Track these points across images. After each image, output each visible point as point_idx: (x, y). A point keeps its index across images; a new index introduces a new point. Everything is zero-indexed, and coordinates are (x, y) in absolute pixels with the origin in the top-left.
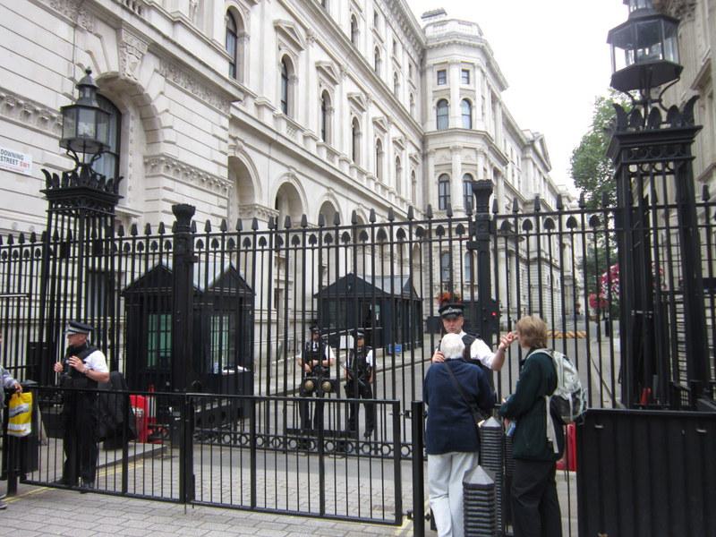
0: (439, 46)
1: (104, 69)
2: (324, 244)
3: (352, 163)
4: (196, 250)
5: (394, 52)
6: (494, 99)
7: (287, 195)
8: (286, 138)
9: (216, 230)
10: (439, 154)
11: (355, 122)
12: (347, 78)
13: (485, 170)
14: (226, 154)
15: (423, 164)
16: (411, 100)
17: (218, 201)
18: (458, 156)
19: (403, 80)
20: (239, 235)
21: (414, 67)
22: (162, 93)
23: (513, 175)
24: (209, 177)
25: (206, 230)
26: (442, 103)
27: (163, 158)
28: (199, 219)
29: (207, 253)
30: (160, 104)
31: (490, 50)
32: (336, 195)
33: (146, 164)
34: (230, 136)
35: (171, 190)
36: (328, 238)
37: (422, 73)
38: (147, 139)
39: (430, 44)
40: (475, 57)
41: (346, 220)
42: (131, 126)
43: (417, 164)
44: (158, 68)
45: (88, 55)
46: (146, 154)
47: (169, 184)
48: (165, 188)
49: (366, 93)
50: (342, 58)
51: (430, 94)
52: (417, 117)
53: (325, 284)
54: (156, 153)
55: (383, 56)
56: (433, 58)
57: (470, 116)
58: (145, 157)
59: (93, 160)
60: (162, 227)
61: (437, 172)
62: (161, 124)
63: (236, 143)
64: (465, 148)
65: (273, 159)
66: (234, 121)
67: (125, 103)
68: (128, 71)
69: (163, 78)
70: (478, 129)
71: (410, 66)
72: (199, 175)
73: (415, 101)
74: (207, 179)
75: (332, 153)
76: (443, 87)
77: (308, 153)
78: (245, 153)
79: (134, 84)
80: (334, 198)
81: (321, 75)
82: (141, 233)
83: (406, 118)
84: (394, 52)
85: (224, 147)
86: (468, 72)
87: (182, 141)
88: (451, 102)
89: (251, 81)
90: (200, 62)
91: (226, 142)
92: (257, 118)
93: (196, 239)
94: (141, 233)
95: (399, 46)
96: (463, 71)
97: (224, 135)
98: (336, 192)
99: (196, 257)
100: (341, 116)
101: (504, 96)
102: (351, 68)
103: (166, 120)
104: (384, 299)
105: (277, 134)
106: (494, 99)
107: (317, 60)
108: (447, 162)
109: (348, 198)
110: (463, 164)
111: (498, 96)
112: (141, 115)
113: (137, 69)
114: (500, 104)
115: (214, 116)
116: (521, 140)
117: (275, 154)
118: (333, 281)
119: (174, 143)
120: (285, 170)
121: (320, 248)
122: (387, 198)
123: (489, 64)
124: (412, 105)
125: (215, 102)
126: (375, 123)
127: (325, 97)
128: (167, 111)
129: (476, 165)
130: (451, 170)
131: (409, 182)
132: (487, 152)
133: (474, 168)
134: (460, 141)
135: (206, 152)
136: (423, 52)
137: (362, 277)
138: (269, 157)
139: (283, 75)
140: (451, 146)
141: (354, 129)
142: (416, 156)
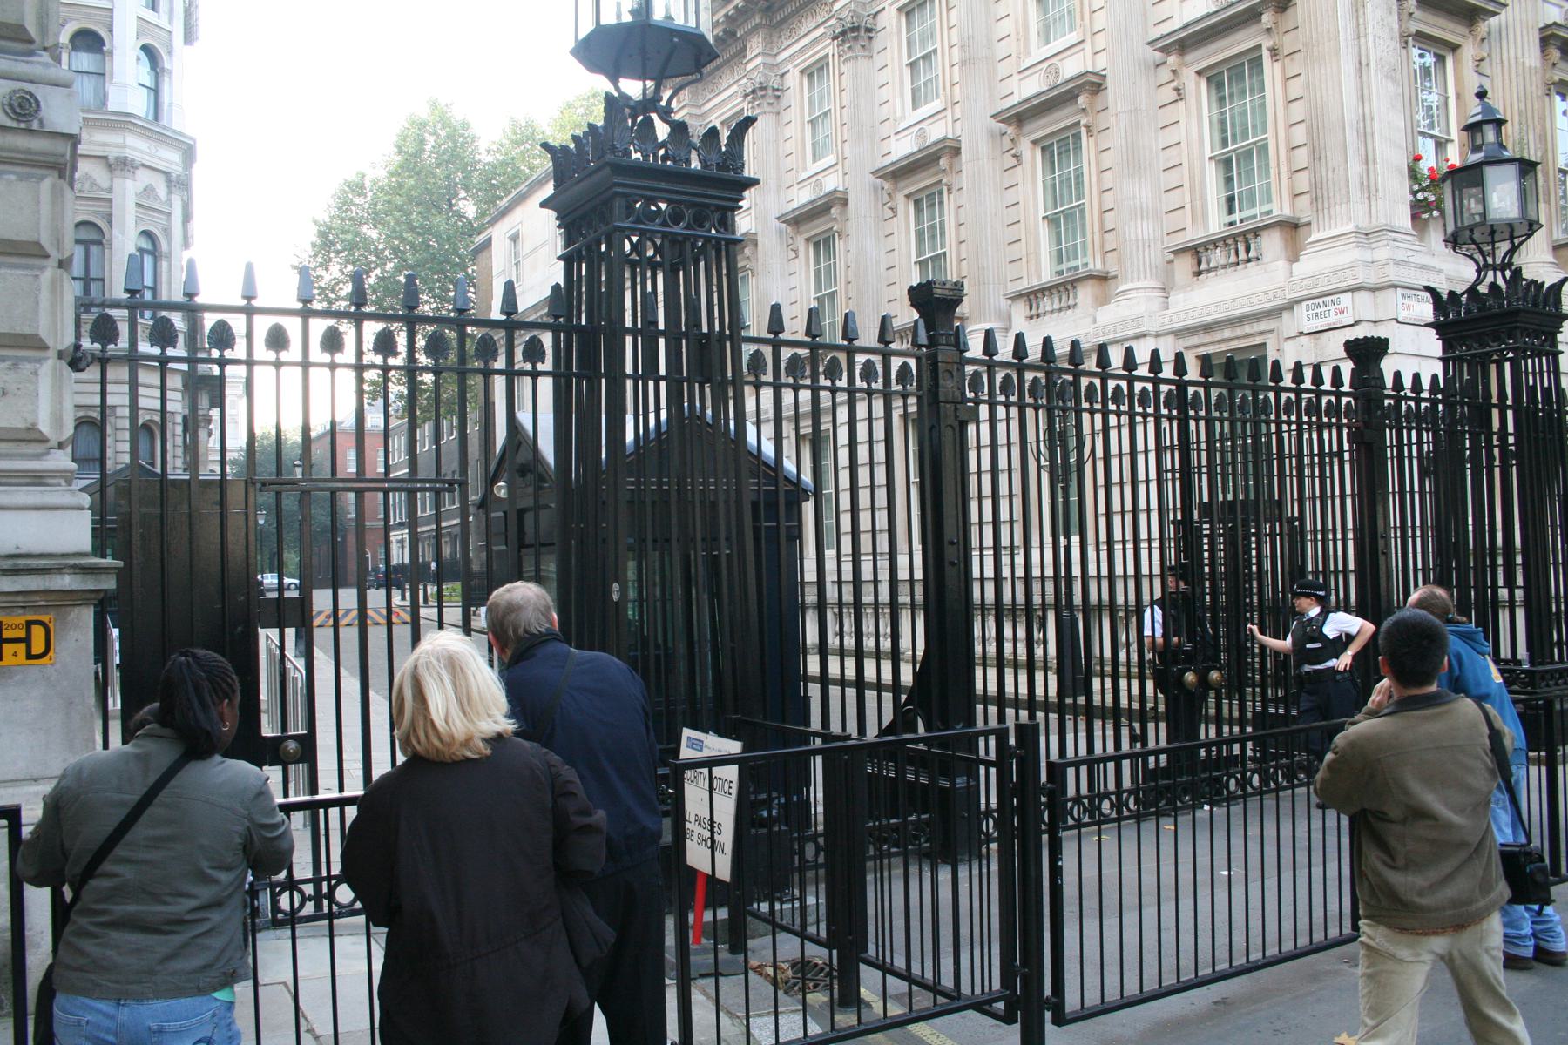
18: (129, 183)
64: (144, 166)
110: (138, 205)
129: (169, 215)
130: (109, 219)
133: (162, 219)
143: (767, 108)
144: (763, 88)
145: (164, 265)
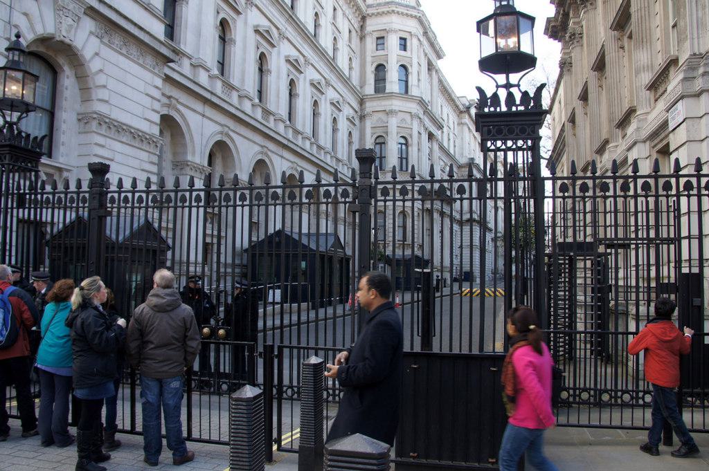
0: (378, 13)
1: (40, 31)
2: (223, 203)
3: (288, 122)
4: (109, 205)
5: (334, 17)
6: (431, 67)
7: (220, 150)
8: (220, 98)
9: (141, 186)
10: (376, 117)
11: (292, 83)
12: (285, 41)
13: (419, 133)
14: (158, 112)
15: (361, 126)
16: (350, 65)
17: (149, 157)
19: (342, 44)
20: (133, 193)
21: (354, 33)
22: (97, 54)
23: (449, 140)
24: (140, 134)
25: (77, 188)
26: (380, 68)
27: (95, 116)
28: (112, 177)
29: (119, 208)
30: (94, 66)
31: (427, 20)
32: (269, 153)
33: (79, 120)
34: (163, 94)
35: (103, 146)
36: (259, 197)
37: (362, 38)
38: (81, 98)
39: (370, 11)
40: (412, 26)
41: (276, 180)
42: (66, 84)
43: (354, 125)
44: (93, 29)
45: (24, 17)
46: (82, 110)
47: (101, 140)
48: (96, 144)
49: (304, 56)
50: (281, 21)
51: (369, 59)
52: (355, 81)
53: (254, 239)
54: (89, 110)
55: (322, 21)
56: (373, 25)
57: (407, 82)
58: (78, 114)
59: (20, 119)
60: (79, 183)
61: (373, 134)
62: (94, 83)
63: (171, 101)
65: (208, 118)
66: (168, 79)
67: (61, 63)
68: (65, 34)
69: (98, 40)
70: (413, 94)
71: (350, 31)
72: (131, 132)
73: (354, 65)
74: (139, 136)
75: (267, 113)
76: (380, 53)
77: (243, 112)
78: (178, 111)
79: (69, 46)
80: (269, 157)
81: (259, 38)
82: (73, 188)
83: (346, 81)
84: (334, 17)
85: (157, 106)
86: (405, 39)
87: (114, 100)
88: (388, 67)
89: (187, 41)
90: (135, 25)
91: (159, 101)
92: (192, 78)
93: (109, 195)
94: (73, 188)
95: (339, 13)
96: (401, 38)
97: (157, 94)
98: (271, 151)
99: (109, 211)
100: (278, 77)
101: (440, 64)
102: (290, 32)
103: (100, 80)
104: (308, 254)
105: (212, 93)
106: (431, 67)
107: (256, 23)
108: (385, 125)
109: (282, 157)
111: (434, 63)
112: (76, 75)
113: (73, 30)
114: (436, 71)
115: (148, 76)
116: (457, 107)
117: (209, 111)
118: (262, 237)
119: (107, 102)
120: (219, 128)
121: (251, 206)
122: (322, 158)
123: (425, 33)
124: (351, 69)
125: (149, 60)
126: (312, 84)
127: (262, 57)
128: (101, 71)
129: (412, 129)
130: (387, 133)
131: (346, 143)
132: (421, 116)
134: (396, 104)
135: (138, 110)
136: (364, 19)
137: (290, 234)
138: (203, 116)
139: (220, 37)
140: (388, 109)
141: (290, 90)
142: (353, 117)
143: (576, 44)
144: (574, 34)
145: (410, 149)
